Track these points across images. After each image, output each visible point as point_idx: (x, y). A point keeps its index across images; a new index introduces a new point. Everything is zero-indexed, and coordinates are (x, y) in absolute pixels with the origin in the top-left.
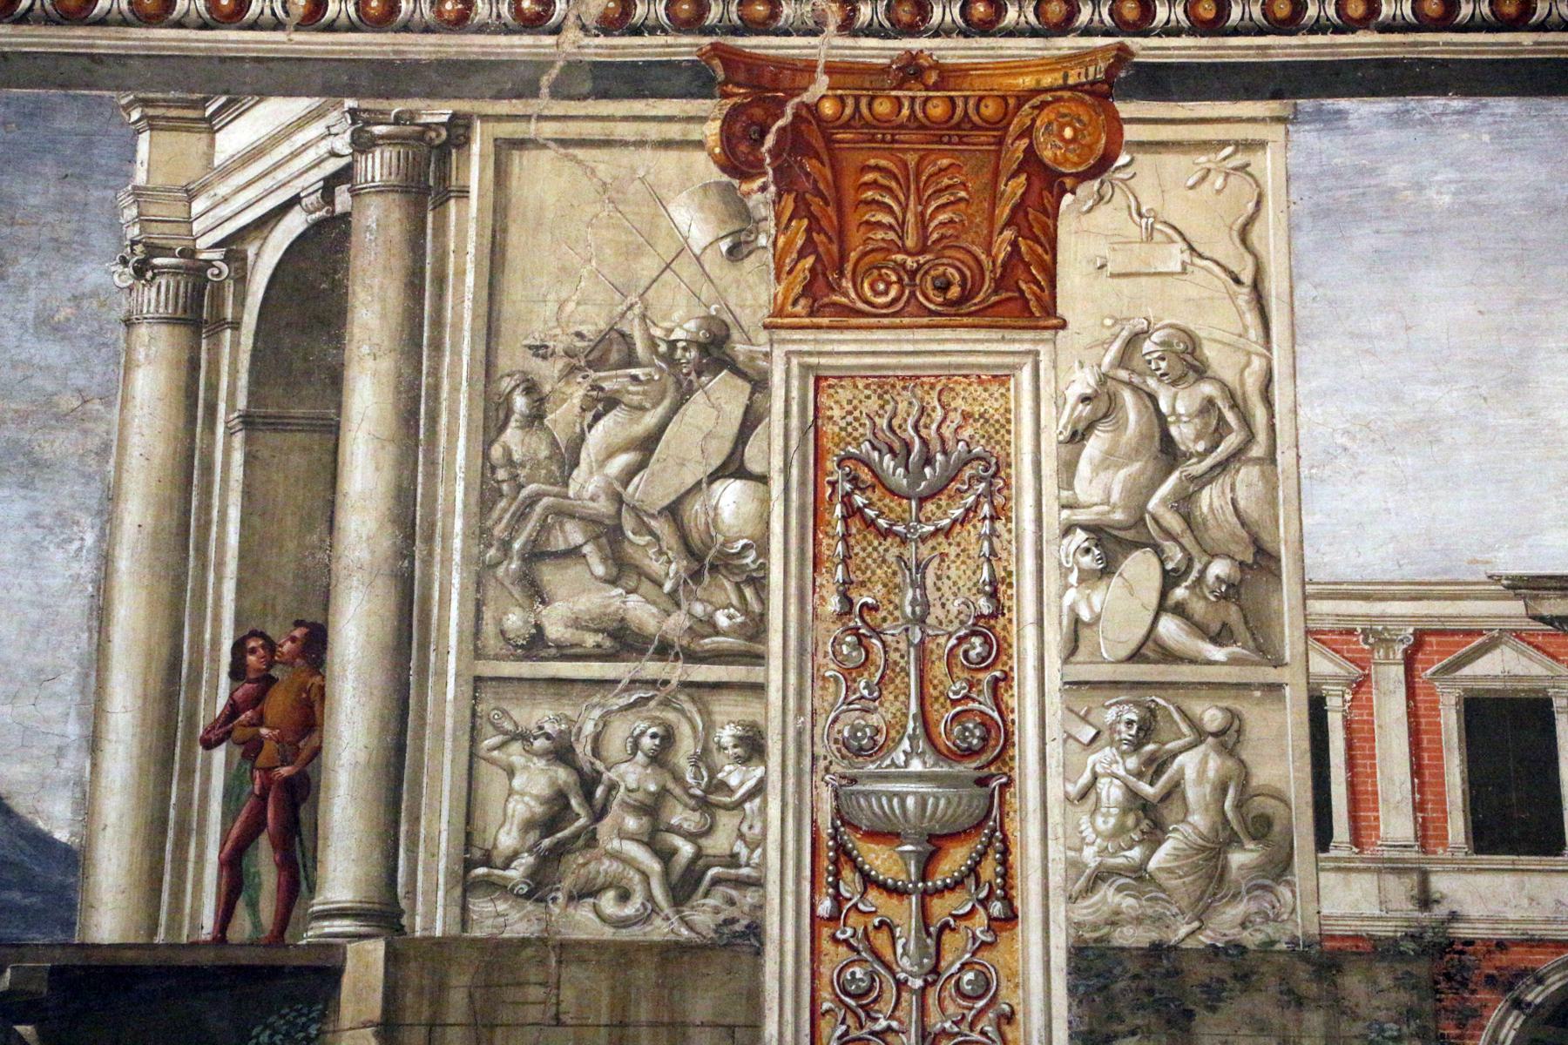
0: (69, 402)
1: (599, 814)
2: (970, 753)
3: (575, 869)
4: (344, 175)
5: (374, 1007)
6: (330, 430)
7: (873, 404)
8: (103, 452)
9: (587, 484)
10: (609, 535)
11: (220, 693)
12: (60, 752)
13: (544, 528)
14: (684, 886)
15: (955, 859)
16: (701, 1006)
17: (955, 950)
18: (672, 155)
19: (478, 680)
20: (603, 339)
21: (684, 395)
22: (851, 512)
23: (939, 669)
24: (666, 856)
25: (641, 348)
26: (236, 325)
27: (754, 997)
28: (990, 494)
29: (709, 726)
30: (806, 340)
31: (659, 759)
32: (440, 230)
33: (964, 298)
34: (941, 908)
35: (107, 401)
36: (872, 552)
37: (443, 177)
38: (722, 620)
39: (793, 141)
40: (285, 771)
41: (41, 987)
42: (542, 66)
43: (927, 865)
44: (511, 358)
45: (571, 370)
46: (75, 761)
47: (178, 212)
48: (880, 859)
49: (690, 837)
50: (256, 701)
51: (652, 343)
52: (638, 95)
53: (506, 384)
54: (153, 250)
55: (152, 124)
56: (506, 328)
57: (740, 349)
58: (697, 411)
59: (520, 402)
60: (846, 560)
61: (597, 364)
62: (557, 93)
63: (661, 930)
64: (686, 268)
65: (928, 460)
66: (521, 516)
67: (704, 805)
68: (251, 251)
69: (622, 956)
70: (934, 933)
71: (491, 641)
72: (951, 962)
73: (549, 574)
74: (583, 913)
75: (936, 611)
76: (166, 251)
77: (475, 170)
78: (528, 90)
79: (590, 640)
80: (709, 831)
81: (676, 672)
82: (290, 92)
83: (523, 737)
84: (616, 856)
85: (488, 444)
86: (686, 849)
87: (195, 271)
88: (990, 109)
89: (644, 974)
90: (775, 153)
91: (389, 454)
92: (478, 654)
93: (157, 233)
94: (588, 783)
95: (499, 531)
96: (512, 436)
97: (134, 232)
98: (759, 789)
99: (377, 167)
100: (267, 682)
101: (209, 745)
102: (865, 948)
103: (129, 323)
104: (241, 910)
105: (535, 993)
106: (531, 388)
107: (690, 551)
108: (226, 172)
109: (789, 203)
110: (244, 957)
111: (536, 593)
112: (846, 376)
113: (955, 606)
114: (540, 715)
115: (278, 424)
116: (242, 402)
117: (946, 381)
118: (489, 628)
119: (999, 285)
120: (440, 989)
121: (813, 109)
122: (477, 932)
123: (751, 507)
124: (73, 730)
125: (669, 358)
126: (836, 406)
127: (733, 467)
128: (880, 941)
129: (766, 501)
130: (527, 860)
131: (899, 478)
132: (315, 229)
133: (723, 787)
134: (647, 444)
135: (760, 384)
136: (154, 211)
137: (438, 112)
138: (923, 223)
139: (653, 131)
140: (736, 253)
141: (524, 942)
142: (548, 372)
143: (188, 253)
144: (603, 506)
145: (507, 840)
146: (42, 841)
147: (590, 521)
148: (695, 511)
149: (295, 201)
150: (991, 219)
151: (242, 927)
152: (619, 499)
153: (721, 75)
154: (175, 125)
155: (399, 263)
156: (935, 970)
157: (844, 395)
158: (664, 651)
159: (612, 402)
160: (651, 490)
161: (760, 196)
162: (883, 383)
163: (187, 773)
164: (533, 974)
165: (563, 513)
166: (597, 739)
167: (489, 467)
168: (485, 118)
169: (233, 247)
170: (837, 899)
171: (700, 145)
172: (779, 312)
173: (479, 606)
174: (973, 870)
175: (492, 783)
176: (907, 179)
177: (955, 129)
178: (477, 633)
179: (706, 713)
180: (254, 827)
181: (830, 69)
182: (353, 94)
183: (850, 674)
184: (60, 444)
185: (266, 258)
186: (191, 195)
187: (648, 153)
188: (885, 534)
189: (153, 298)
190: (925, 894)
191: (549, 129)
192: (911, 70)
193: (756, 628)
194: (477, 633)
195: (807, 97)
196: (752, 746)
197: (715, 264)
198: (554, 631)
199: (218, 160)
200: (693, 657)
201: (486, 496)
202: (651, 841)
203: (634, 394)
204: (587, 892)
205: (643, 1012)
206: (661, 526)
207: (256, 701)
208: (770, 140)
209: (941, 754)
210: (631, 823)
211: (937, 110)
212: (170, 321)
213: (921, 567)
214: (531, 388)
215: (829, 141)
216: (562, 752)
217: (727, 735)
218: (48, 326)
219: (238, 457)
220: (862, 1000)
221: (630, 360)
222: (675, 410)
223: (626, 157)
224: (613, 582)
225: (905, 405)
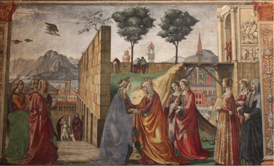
0: (214, 27)
1: (249, 54)
2: (271, 50)
3: (248, 58)
4: (230, 11)
5: (236, 67)
6: (230, 29)
7: (264, 27)
8: (217, 30)
9: (247, 32)
10: (248, 36)
11: (225, 47)
12: (216, 50)
13: (244, 35)
14: (254, 59)
15: (271, 57)
16: (256, 67)
17: (271, 63)
18: (251, 9)
19: (241, 46)
20: (247, 22)
21: (252, 26)
22: (263, 34)
23: (269, 45)
24: (253, 57)
25: (249, 23)
26: (224, 21)
27: (259, 66)
28: (272, 33)
29: (255, 49)
30: (260, 22)
31: (252, 51)
32: (236, 15)
33: (270, 19)
34: (270, 60)
35: (217, 27)
36: (265, 37)
37: (236, 11)
38: (256, 41)
39: (258, 8)
40: (230, 52)
41: (217, 65)
42: (242, 3)
43: (269, 57)
44: (241, 24)
45: (245, 24)
46: (217, 51)
47: (220, 14)
48: (266, 57)
49: (255, 56)
50: (228, 47)
51: (250, 22)
52: (248, 5)
53: (241, 25)
54: (219, 16)
55: (218, 7)
56: (241, 21)
57: (256, 23)
58: (253, 27)
59: (242, 27)
60: (263, 37)
61: (247, 24)
62: (243, 5)
63: (253, 62)
64: (252, 17)
65: (268, 30)
66: (243, 34)
67: (255, 54)
68: (224, 16)
69: (251, 63)
70: (270, 62)
71: (242, 43)
72: (271, 64)
73: (245, 38)
74: (248, 61)
75: (269, 41)
76: (219, 16)
77: (238, 10)
78: (241, 5)
79: (248, 43)
80: (256, 55)
81: (253, 45)
82: (226, 5)
83: (244, 49)
84: (250, 57)
85: (240, 29)
86: (254, 57)
87: (221, 18)
88: (271, 6)
89: (252, 65)
90: (257, 9)
91: (234, 30)
92: (241, 44)
93: (219, 15)
94: (248, 52)
95: (242, 35)
96: (242, 29)
97: (217, 15)
98: (258, 53)
99: (232, 10)
100: (228, 46)
101: (225, 50)
102: (265, 63)
103: (218, 21)
104: (228, 60)
105: (246, 66)
106: (243, 26)
107: (254, 37)
108: (223, 11)
109: (258, 13)
110: (228, 63)
111: (244, 40)
112: (263, 24)
113: (270, 40)
114: (245, 48)
115: (227, 28)
116: (225, 27)
117: (269, 25)
118: (241, 42)
119: (272, 18)
120: (240, 66)
121: (259, 6)
122: (242, 62)
123: (257, 34)
124: (217, 49)
125: (251, 24)
126: (262, 26)
127: (256, 31)
128: (266, 62)
129: (258, 33)
130: (245, 57)
131: (266, 32)
132: (229, 14)
133: (256, 52)
134: (250, 29)
135: (257, 25)
136: (218, 13)
137: (235, 6)
138: (267, 14)
139: (250, 7)
140: (255, 16)
141: (245, 63)
142: (244, 24)
143: (221, 16)
144: (248, 34)
145: (243, 56)
146: (216, 56)
147: (247, 35)
148: (254, 34)
149: (227, 13)
150: (271, 13)
151: (228, 62)
152: (249, 33)
153: (253, 3)
154: (219, 7)
155: (234, 17)
156: (270, 64)
157: (262, 26)
158: (252, 43)
159: (248, 27)
160: (251, 32)
161: (256, 12)
162: (265, 25)
163: (224, 52)
164: (246, 65)
165: (245, 34)
166: (248, 49)
167: (241, 31)
168: (239, 7)
169: (223, 16)
170: (264, 60)
171: (252, 8)
172: (258, 20)
173: (241, 41)
174: (272, 58)
175: (242, 52)
176: (266, 11)
177: (269, 7)
178: (241, 42)
179: (255, 48)
180: (228, 55)
181: (261, 3)
182: (230, 5)
183: (264, 45)
184: (214, 30)
185: (226, 16)
186: (221, 12)
187: (249, 9)
188: (265, 35)
189: (219, 20)
190: (269, 59)
191: (243, 7)
192: (266, 3)
193: (258, 42)
194: (241, 42)
195: (259, 5)
196: (258, 50)
197: (254, 17)
198: (245, 42)
199: (222, 10)
200: (254, 44)
201: (241, 33)
202: (252, 56)
203: (249, 26)
204: (249, 59)
205: (252, 67)
206: (251, 35)
207: (228, 47)
208: (257, 8)
209: (270, 50)
210: (251, 55)
211: (267, 6)
212: (220, 21)
213: (268, 38)
214: (243, 26)
215: (261, 8)
216: (246, 50)
217: (256, 49)
218: (213, 22)
219: (225, 31)
220: (265, 66)
221: (249, 24)
222: (252, 27)
223: (248, 9)
224: (249, 39)
225: (266, 26)
